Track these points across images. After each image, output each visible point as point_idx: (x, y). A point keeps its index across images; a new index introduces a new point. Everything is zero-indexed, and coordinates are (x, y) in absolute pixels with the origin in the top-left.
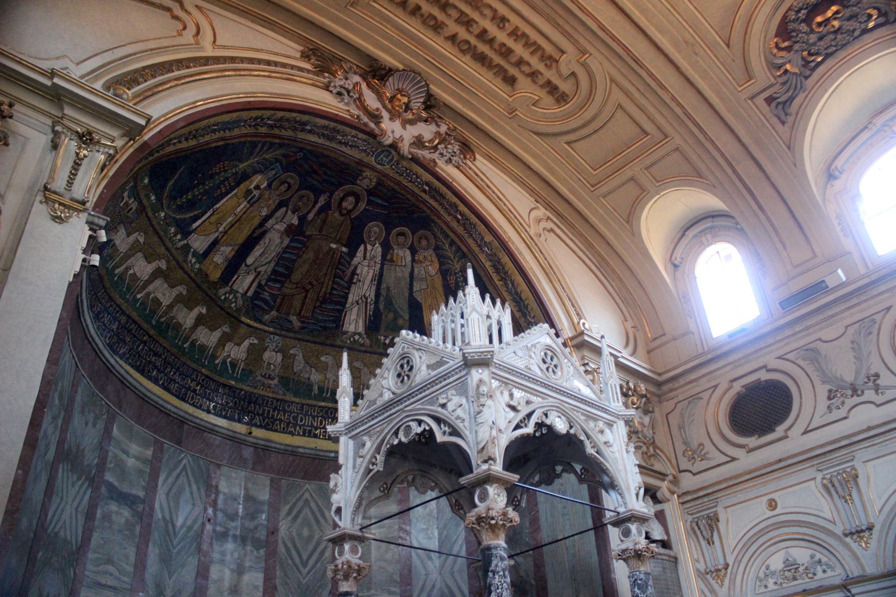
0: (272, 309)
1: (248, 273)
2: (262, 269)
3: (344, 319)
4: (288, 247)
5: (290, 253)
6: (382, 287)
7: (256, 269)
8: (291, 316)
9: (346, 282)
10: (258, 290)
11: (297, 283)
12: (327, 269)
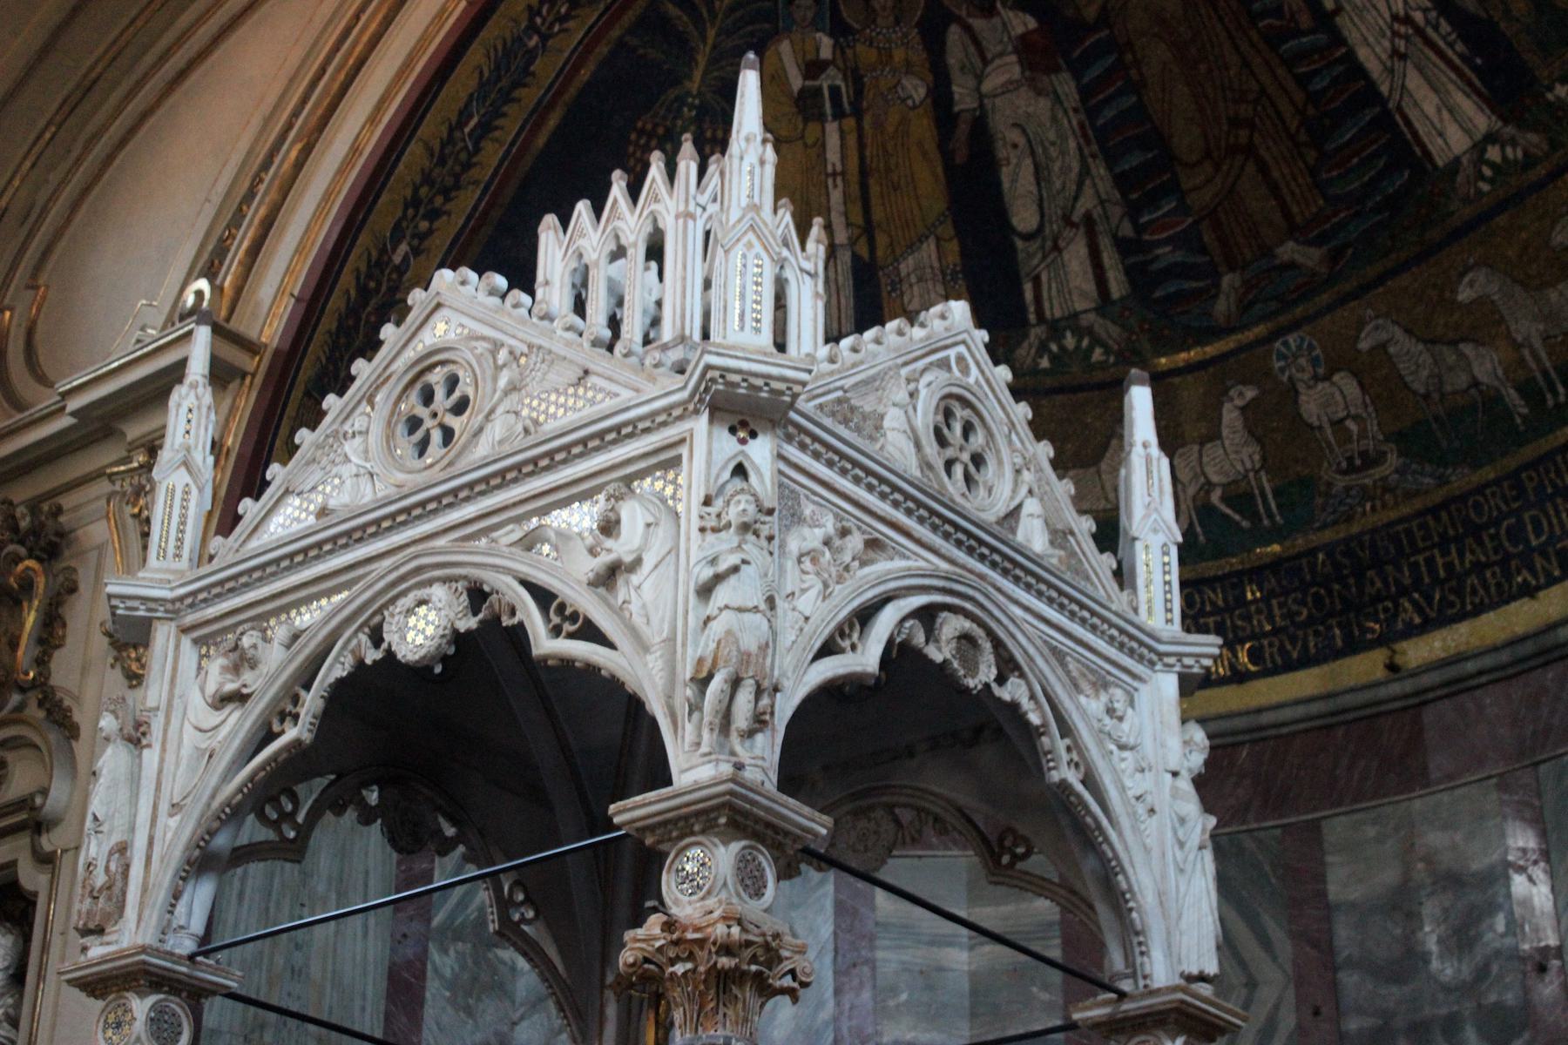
0: (1216, 276)
1: (1056, 248)
2: (1086, 203)
3: (1415, 134)
4: (1085, 93)
5: (1107, 101)
7: (1067, 220)
8: (1280, 251)
9: (1312, 31)
10: (1132, 260)
11: (1208, 154)
12: (1237, 48)
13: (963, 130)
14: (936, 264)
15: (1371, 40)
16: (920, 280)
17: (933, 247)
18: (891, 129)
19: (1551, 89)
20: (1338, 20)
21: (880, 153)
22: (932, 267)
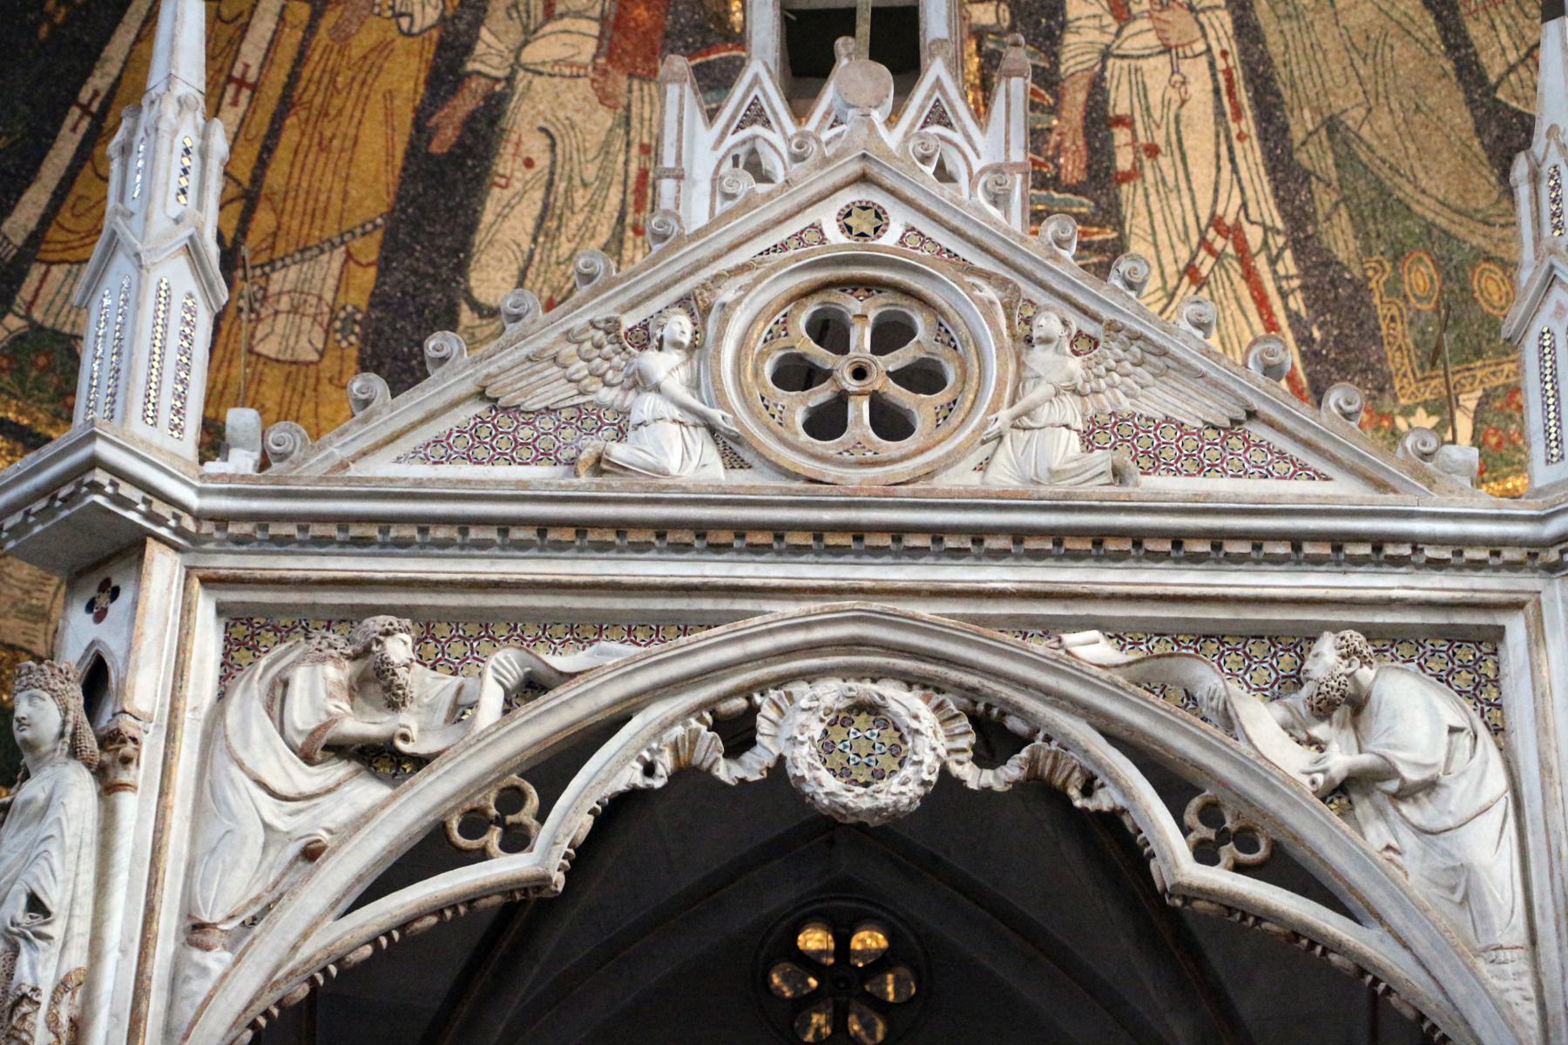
6: (1297, 134)
9: (1075, 190)
13: (465, 103)
14: (328, 296)
15: (1162, 237)
16: (294, 310)
17: (336, 266)
18: (356, 53)
19: (1408, 412)
20: (1125, 187)
21: (326, 80)
22: (320, 298)
